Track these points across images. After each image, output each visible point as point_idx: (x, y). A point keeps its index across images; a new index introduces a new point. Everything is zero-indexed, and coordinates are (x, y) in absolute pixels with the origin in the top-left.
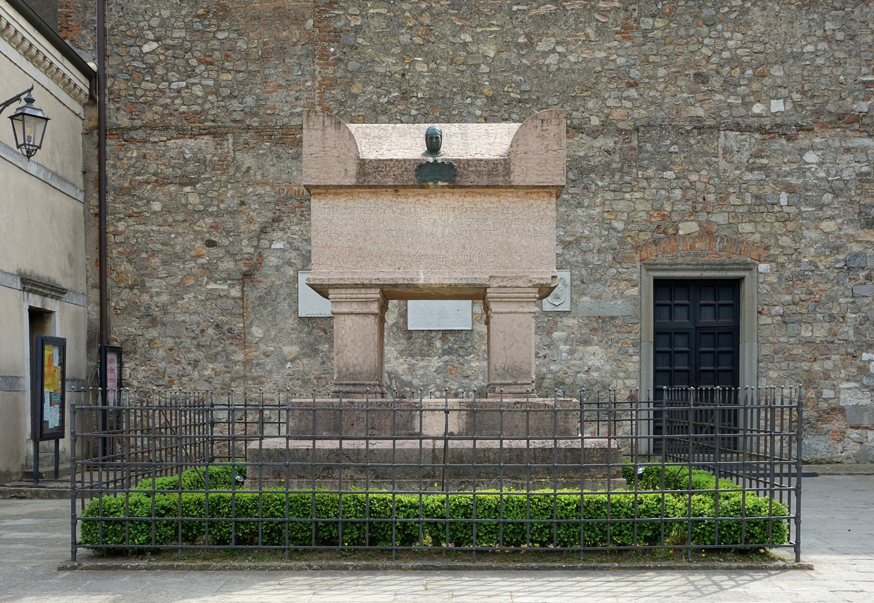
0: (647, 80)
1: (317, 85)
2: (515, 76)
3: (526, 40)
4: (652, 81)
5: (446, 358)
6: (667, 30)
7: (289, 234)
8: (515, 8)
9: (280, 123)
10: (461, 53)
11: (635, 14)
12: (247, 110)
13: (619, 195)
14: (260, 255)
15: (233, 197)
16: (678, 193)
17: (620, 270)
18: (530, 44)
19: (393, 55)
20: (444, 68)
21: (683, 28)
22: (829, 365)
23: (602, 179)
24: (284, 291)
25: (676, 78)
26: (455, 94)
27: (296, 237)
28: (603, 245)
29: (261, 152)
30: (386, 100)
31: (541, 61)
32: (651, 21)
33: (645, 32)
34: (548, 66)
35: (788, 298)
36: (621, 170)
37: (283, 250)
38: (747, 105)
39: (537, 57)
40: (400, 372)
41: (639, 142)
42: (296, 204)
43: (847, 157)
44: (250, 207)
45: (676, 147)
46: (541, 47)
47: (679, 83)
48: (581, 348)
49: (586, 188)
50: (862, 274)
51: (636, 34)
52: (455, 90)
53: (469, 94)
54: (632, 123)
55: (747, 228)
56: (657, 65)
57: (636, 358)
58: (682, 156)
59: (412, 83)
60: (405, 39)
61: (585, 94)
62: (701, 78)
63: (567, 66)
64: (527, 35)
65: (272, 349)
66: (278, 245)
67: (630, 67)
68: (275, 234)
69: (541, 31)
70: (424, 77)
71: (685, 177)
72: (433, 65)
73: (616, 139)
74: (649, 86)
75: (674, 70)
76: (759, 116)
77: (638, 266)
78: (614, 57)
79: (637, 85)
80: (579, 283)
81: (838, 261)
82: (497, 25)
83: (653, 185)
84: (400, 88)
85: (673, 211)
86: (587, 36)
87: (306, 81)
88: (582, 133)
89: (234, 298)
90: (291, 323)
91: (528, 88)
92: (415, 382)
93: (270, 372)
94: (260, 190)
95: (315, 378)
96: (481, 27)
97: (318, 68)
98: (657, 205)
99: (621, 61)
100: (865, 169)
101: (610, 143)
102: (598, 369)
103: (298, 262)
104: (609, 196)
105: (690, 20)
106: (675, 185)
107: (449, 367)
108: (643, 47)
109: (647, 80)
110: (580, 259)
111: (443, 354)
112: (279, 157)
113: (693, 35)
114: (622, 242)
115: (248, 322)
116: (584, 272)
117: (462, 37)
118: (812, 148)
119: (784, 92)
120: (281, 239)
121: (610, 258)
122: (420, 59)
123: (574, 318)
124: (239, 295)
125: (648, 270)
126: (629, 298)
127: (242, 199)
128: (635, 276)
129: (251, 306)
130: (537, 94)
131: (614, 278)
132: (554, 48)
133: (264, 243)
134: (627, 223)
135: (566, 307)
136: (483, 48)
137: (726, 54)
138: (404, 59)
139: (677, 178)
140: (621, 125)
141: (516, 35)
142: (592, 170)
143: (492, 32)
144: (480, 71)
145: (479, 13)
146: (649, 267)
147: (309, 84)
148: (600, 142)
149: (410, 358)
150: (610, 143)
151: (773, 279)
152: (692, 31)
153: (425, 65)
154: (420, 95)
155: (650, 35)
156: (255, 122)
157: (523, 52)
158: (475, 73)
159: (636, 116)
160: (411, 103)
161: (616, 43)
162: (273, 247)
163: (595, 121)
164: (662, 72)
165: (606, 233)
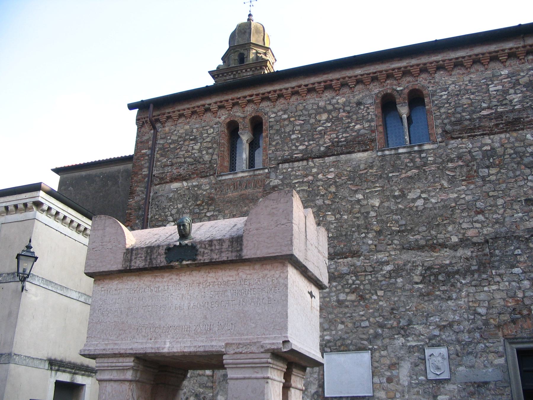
0: (490, 208)
2: (394, 216)
3: (400, 193)
4: (494, 208)
6: (500, 174)
8: (390, 175)
10: (356, 206)
11: (475, 168)
13: (480, 289)
17: (487, 344)
18: (403, 195)
20: (346, 217)
21: (511, 172)
23: (464, 278)
25: (512, 204)
26: (354, 232)
28: (471, 326)
31: (412, 205)
32: (486, 170)
33: (483, 178)
34: (417, 207)
36: (478, 271)
39: (409, 202)
41: (490, 250)
45: (519, 250)
46: (411, 196)
47: (514, 207)
49: (453, 285)
51: (477, 180)
52: (353, 229)
53: (363, 231)
54: (482, 238)
56: (496, 198)
58: (525, 256)
60: (319, 202)
61: (445, 222)
63: (431, 206)
64: (401, 190)
67: (476, 201)
69: (410, 186)
70: (332, 224)
72: (338, 216)
73: (472, 249)
74: (492, 212)
75: (508, 199)
77: (502, 341)
78: (463, 196)
79: (483, 212)
80: (454, 356)
83: (505, 279)
85: (524, 297)
86: (442, 185)
88: (446, 248)
89: (208, 376)
91: (404, 222)
96: (369, 189)
98: (511, 294)
101: (468, 253)
104: (472, 290)
105: (515, 166)
106: (523, 278)
108: (484, 187)
109: (490, 208)
110: (454, 338)
113: (519, 175)
114: (486, 323)
115: (215, 392)
116: (458, 348)
117: (357, 197)
121: (477, 335)
122: (330, 213)
123: (454, 384)
125: (511, 343)
128: (501, 349)
129: (218, 381)
130: (411, 226)
132: (420, 196)
134: (488, 308)
135: (446, 376)
136: (371, 202)
139: (524, 272)
140: (475, 240)
141: (393, 191)
142: (457, 272)
143: (376, 191)
144: (370, 216)
145: (367, 181)
146: (511, 340)
148: (460, 252)
150: (468, 253)
152: (518, 173)
153: (333, 217)
155: (487, 179)
157: (399, 201)
158: (366, 218)
159: (485, 232)
164: (500, 202)
165: (473, 317)
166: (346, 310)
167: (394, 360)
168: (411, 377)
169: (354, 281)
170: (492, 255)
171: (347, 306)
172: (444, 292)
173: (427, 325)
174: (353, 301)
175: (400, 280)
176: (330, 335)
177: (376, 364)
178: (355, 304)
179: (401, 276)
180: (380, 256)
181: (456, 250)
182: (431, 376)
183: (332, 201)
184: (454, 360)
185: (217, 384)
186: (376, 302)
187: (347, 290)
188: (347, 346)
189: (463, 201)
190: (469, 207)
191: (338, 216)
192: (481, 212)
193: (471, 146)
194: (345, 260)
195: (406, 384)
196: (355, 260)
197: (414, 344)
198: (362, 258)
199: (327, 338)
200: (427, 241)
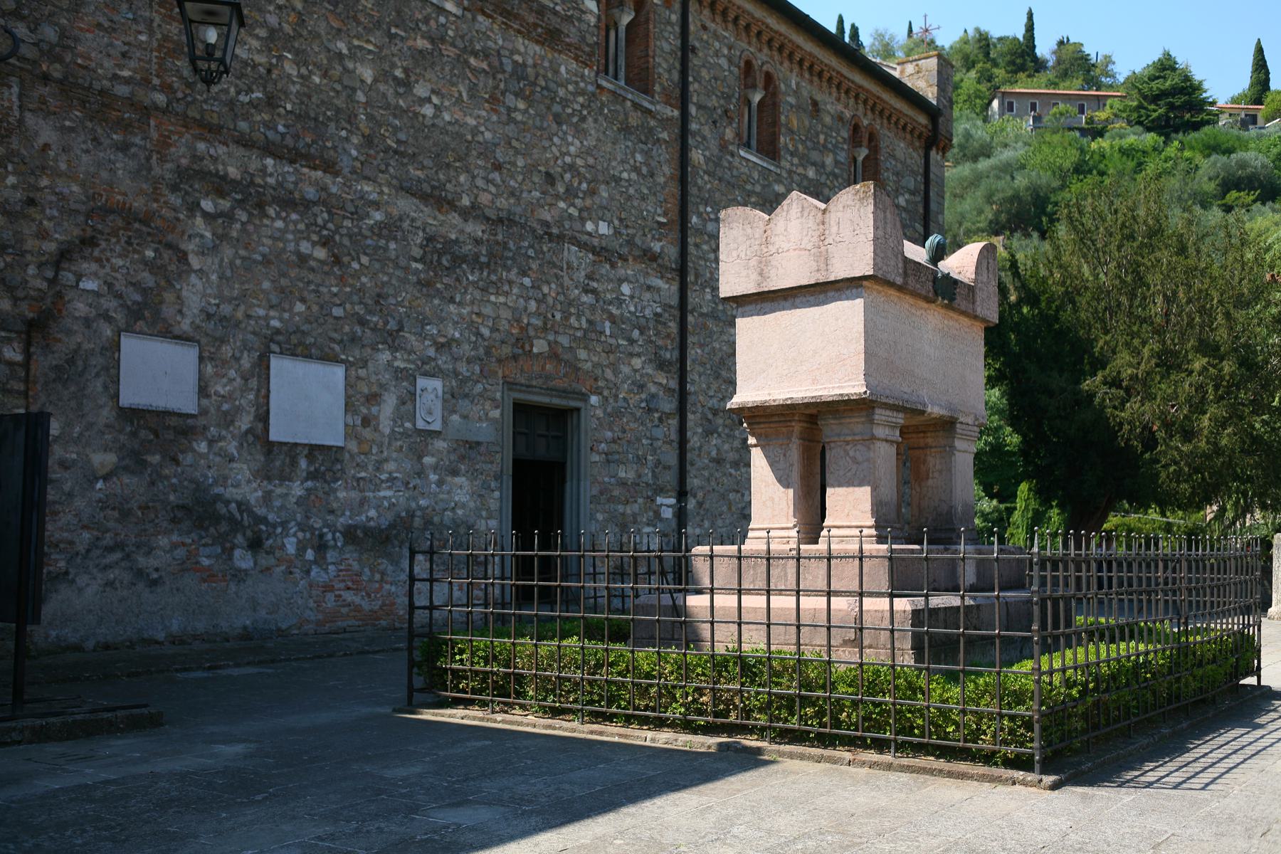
1: (155, 44)
5: (309, 484)
7: (108, 269)
8: (393, 30)
9: (97, 85)
12: (45, 47)
14: (59, 295)
15: (14, 187)
16: (533, 305)
18: (406, 84)
19: (257, 37)
20: (317, 80)
22: (636, 507)
23: (472, 273)
24: (97, 361)
27: (119, 276)
29: (67, 123)
30: (247, 99)
31: (418, 109)
35: (609, 434)
36: (488, 265)
37: (97, 294)
38: (583, 220)
40: (253, 502)
42: (120, 223)
43: (647, 296)
44: (43, 211)
48: (449, 479)
49: (458, 280)
50: (656, 415)
52: (329, 113)
55: (582, 354)
56: (517, 152)
57: (497, 494)
59: (279, 86)
62: (550, 179)
64: (406, 70)
65: (74, 456)
66: (90, 285)
68: (85, 265)
71: (539, 288)
76: (589, 234)
81: (642, 401)
82: (375, 45)
84: (265, 87)
85: (528, 324)
87: (140, 33)
90: (106, 414)
92: (271, 517)
93: (70, 495)
94: (61, 186)
95: (140, 508)
97: (157, 19)
99: (488, 135)
100: (659, 310)
102: (464, 506)
103: (119, 317)
107: (313, 497)
111: (307, 479)
112: (95, 139)
118: (626, 280)
119: (608, 215)
120: (96, 274)
122: (289, 56)
123: (444, 440)
124: (19, 358)
126: (488, 420)
127: (31, 195)
128: (498, 395)
131: (481, 395)
133: (67, 277)
135: (437, 426)
137: (568, 159)
138: (270, 50)
141: (393, 66)
146: (510, 385)
147: (143, 38)
149: (265, 482)
151: (599, 413)
154: (289, 107)
156: (56, 70)
158: (351, 98)
160: (279, 115)
161: (484, 113)
162: (81, 285)
163: (466, 201)
166: (311, 277)
167: (375, 389)
168: (394, 420)
169: (326, 222)
170: (505, 246)
171: (312, 270)
172: (447, 286)
173: (422, 336)
174: (322, 262)
175: (392, 245)
176: (281, 319)
177: (351, 392)
178: (326, 268)
179: (395, 239)
180: (366, 188)
181: (466, 221)
182: (420, 424)
183: (294, 30)
184: (451, 399)
185: (39, 387)
186: (356, 275)
187: (315, 238)
188: (308, 347)
189: (480, 139)
190: (487, 151)
191: (304, 71)
192: (498, 167)
193: (500, 42)
194: (313, 173)
195: (387, 431)
196: (328, 179)
197: (402, 366)
198: (339, 179)
199: (275, 323)
200: (433, 188)
